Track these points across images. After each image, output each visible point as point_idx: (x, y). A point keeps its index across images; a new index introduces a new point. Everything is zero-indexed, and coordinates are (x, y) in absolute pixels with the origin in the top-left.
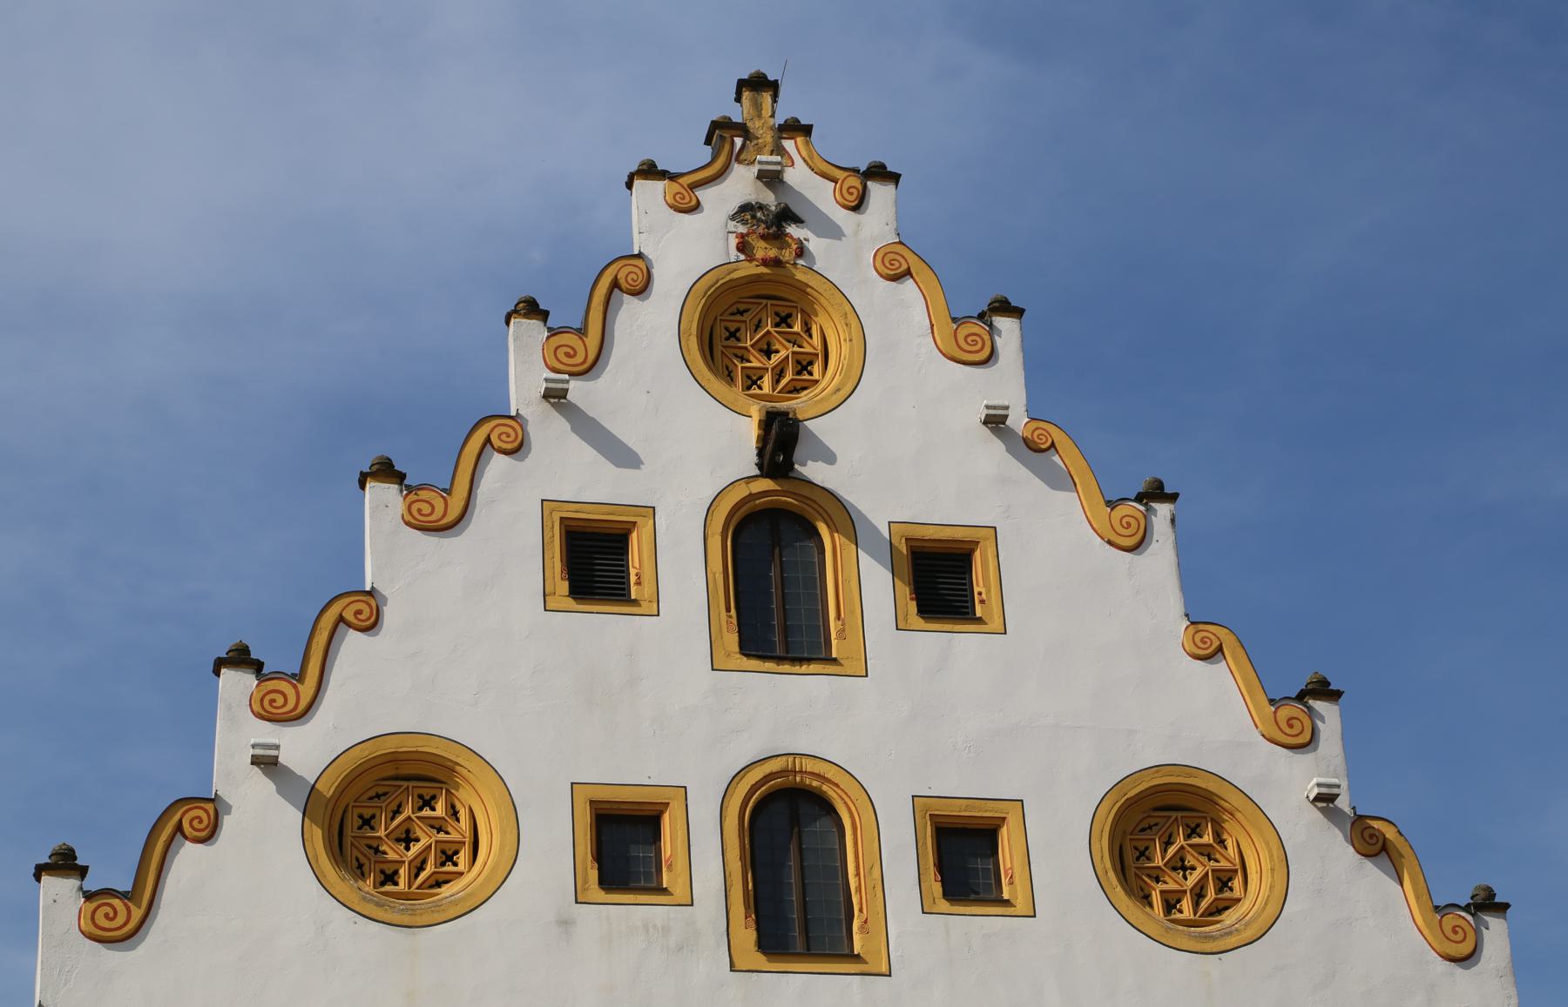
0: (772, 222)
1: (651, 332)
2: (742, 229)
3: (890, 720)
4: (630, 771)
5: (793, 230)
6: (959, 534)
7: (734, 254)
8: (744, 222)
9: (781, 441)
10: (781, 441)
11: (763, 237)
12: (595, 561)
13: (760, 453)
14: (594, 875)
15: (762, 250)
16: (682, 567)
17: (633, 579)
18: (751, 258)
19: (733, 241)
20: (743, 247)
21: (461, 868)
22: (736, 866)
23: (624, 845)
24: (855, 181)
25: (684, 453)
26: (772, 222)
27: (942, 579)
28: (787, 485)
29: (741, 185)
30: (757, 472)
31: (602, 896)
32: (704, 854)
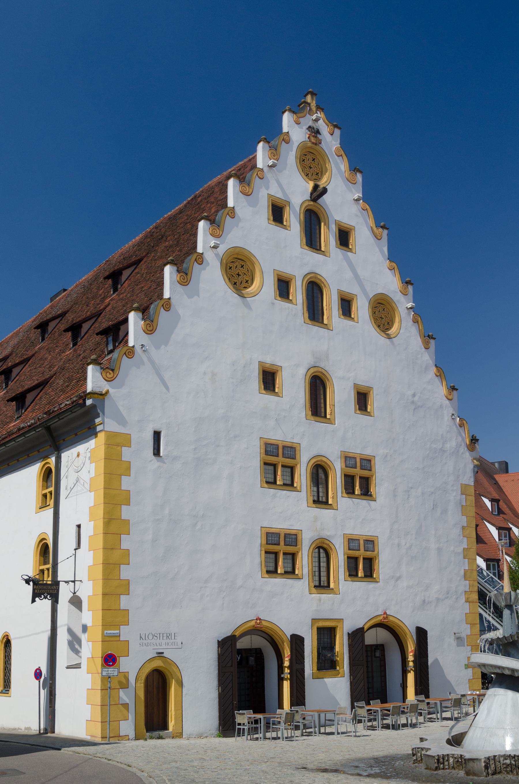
0: (315, 132)
1: (290, 156)
2: (309, 133)
3: (332, 268)
4: (288, 270)
5: (318, 136)
6: (348, 226)
7: (307, 139)
8: (309, 131)
9: (318, 193)
10: (318, 193)
11: (313, 136)
12: (277, 213)
13: (311, 194)
14: (278, 293)
16: (294, 220)
17: (285, 220)
18: (310, 141)
19: (308, 136)
20: (309, 138)
21: (249, 285)
22: (305, 298)
23: (283, 287)
24: (332, 127)
25: (297, 190)
28: (316, 204)
29: (308, 120)
30: (310, 199)
31: (279, 299)
32: (298, 293)
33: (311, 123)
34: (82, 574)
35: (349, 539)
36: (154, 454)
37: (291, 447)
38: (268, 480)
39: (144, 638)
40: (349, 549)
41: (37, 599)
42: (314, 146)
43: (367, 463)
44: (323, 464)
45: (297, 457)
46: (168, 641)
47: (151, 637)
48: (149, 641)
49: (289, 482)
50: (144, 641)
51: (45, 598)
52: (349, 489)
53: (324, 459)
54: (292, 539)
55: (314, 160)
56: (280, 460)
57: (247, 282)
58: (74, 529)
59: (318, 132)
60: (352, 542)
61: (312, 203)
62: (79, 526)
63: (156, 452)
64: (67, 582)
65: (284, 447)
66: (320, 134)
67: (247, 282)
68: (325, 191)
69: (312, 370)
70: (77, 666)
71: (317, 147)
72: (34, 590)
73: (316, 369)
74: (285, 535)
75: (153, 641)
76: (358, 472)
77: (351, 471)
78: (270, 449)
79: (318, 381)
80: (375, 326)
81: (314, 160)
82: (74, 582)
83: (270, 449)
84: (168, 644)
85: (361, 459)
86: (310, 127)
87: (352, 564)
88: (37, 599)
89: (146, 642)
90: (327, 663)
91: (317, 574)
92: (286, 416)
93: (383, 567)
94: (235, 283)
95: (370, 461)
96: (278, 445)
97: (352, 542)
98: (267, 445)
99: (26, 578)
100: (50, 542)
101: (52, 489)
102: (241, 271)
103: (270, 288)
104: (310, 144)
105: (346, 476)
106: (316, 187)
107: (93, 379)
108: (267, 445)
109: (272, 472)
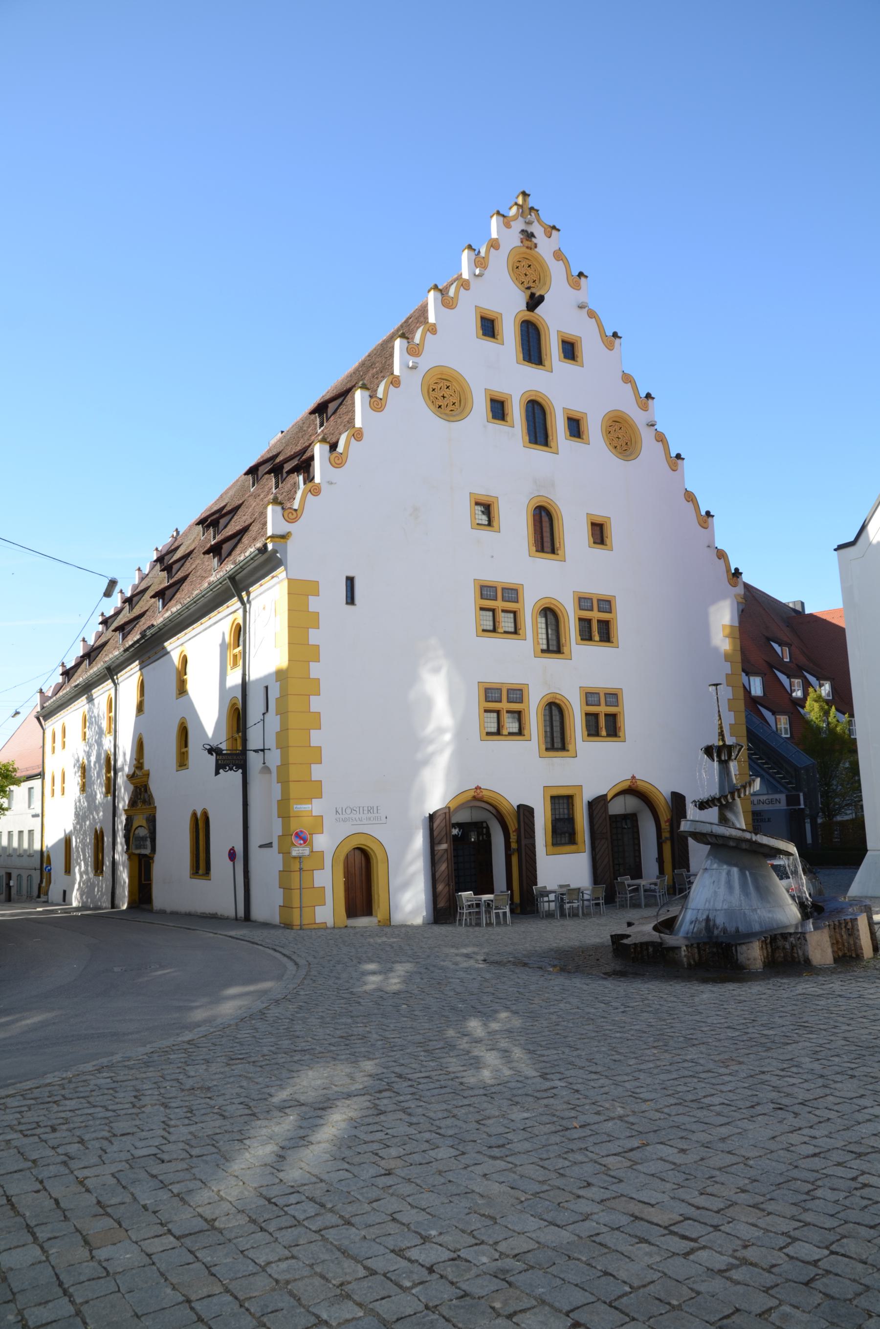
0: (528, 236)
1: (499, 263)
5: (533, 239)
7: (519, 244)
9: (534, 302)
10: (534, 302)
12: (489, 327)
15: (527, 243)
16: (509, 331)
26: (528, 236)
27: (570, 350)
33: (523, 227)
34: (271, 743)
35: (586, 693)
36: (347, 603)
37: (512, 589)
38: (485, 628)
39: (340, 811)
40: (587, 704)
41: (221, 771)
42: (528, 251)
43: (606, 604)
44: (552, 606)
45: (520, 599)
46: (370, 815)
47: (349, 811)
48: (347, 816)
49: (512, 630)
50: (341, 816)
51: (231, 769)
52: (586, 635)
53: (553, 602)
54: (517, 694)
55: (529, 266)
56: (499, 604)
57: (454, 404)
58: (263, 691)
59: (532, 235)
60: (590, 697)
61: (528, 313)
62: (267, 688)
63: (349, 601)
64: (256, 751)
65: (503, 589)
66: (534, 237)
67: (454, 404)
68: (541, 299)
69: (535, 500)
70: (269, 845)
71: (532, 252)
72: (217, 761)
73: (539, 499)
74: (508, 690)
75: (352, 815)
76: (595, 615)
77: (586, 614)
78: (486, 591)
79: (543, 514)
80: (611, 448)
81: (529, 266)
82: (263, 750)
83: (486, 591)
84: (370, 819)
85: (599, 600)
86: (523, 231)
87: (592, 720)
88: (221, 771)
89: (343, 817)
90: (563, 833)
91: (549, 734)
92: (508, 554)
93: (629, 723)
94: (440, 407)
95: (609, 602)
96: (496, 587)
97: (590, 697)
98: (482, 587)
99: (208, 747)
100: (240, 706)
101: (241, 648)
102: (447, 393)
103: (480, 407)
104: (524, 249)
105: (580, 619)
106: (532, 295)
107: (273, 520)
108: (482, 587)
109: (491, 618)
